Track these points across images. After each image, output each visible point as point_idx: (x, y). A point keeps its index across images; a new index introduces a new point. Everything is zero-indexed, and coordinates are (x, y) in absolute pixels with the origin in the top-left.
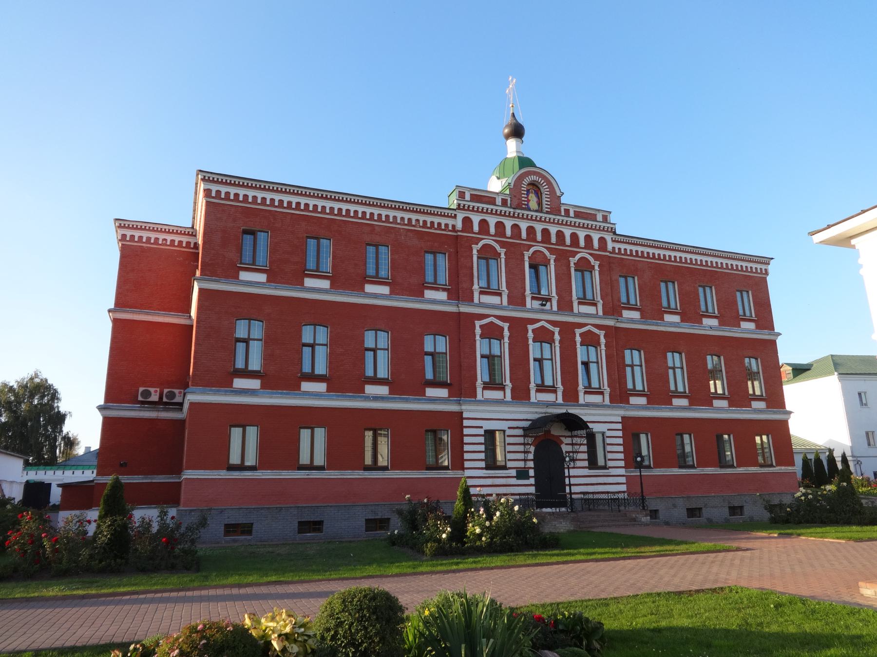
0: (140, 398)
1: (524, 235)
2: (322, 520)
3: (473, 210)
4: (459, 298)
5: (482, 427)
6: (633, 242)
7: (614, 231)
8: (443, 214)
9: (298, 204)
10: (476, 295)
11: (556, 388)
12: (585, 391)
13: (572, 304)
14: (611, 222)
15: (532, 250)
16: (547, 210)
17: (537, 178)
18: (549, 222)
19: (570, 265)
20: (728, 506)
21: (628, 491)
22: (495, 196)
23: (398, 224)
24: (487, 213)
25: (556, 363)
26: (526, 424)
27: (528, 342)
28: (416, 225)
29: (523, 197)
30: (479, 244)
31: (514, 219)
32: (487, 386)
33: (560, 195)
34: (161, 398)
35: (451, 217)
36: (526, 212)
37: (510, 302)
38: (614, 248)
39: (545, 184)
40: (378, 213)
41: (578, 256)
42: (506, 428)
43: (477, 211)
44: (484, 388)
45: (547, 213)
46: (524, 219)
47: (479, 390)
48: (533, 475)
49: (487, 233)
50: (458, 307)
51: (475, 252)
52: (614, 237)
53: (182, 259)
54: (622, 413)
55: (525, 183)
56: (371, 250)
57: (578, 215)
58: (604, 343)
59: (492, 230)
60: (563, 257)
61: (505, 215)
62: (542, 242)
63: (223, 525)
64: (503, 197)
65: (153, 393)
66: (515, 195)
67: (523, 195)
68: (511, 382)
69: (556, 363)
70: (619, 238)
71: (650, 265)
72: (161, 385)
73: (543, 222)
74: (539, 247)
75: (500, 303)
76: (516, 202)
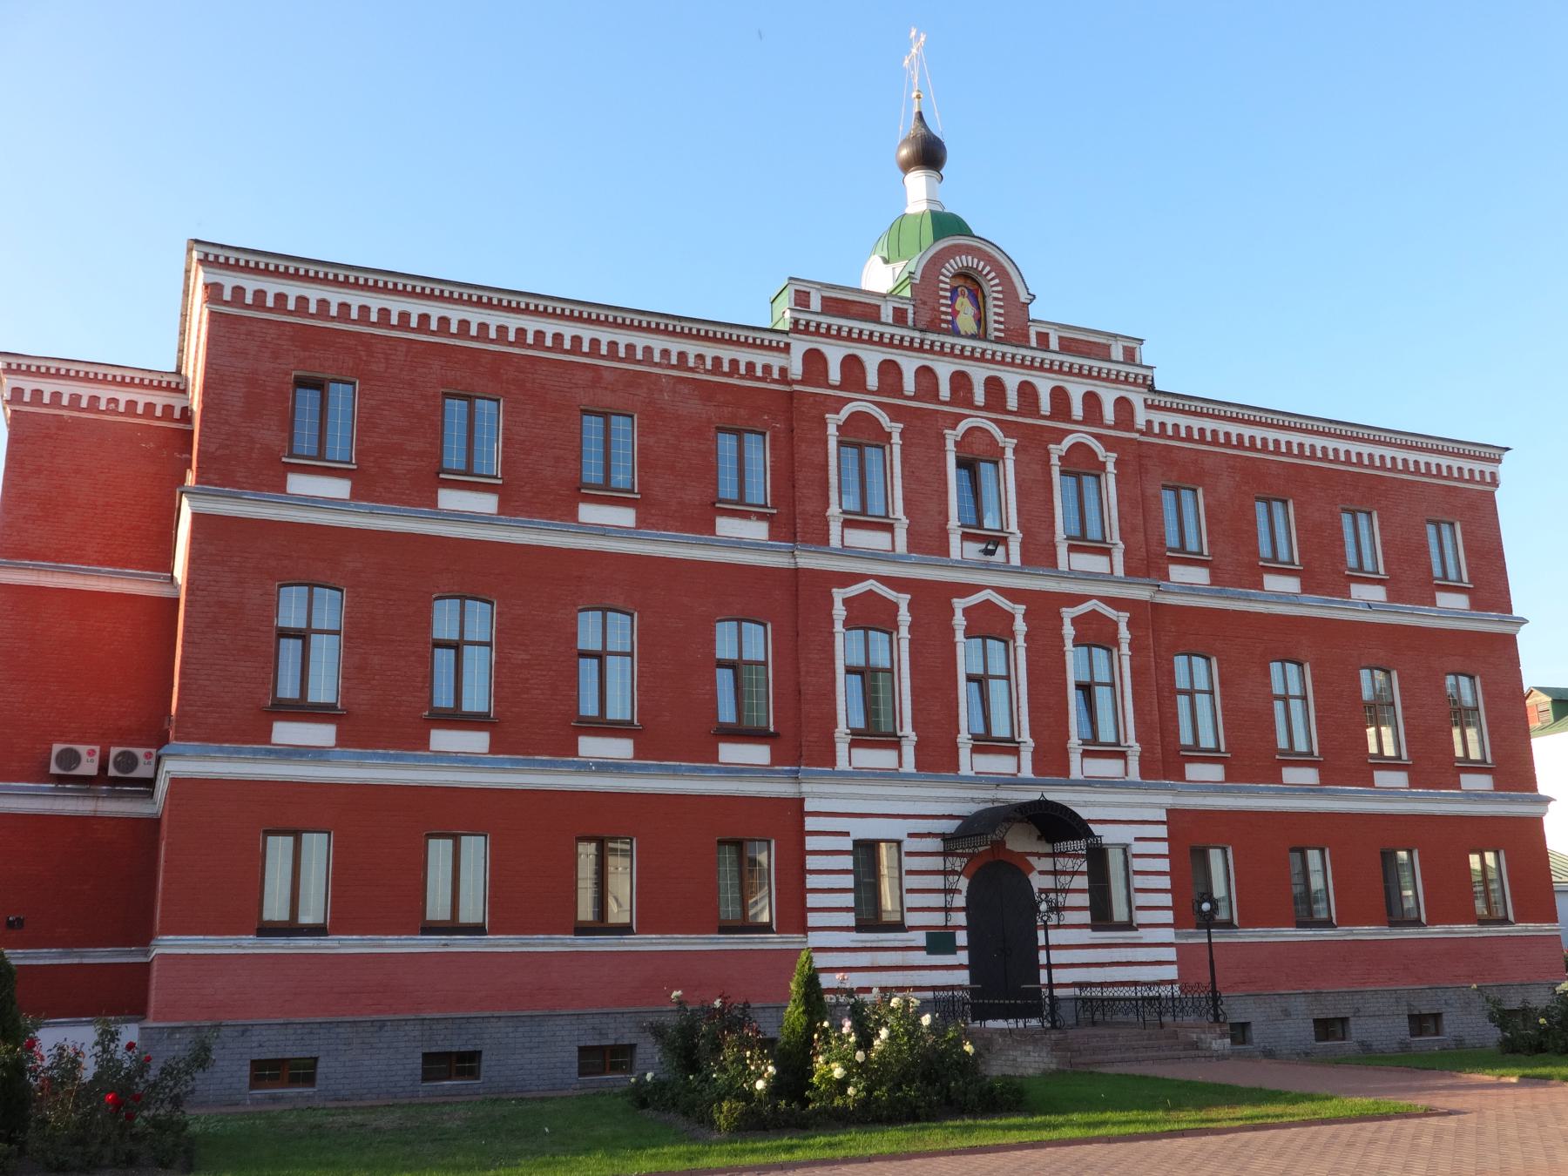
0: (54, 769)
1: (945, 391)
2: (479, 1049)
3: (828, 335)
4: (795, 536)
5: (847, 834)
6: (1193, 409)
7: (1149, 383)
8: (758, 342)
9: (424, 318)
10: (835, 529)
11: (1019, 743)
12: (1084, 750)
13: (1055, 550)
14: (1144, 364)
15: (963, 426)
16: (997, 334)
17: (976, 261)
18: (1003, 362)
19: (1049, 461)
20: (1407, 1012)
21: (1183, 981)
22: (878, 303)
23: (656, 365)
24: (860, 340)
25: (1017, 686)
26: (950, 826)
27: (954, 637)
28: (696, 368)
29: (943, 305)
30: (842, 412)
31: (921, 355)
32: (860, 739)
33: (1028, 301)
34: (103, 767)
35: (777, 349)
36: (949, 340)
37: (912, 546)
38: (1149, 423)
39: (993, 274)
40: (609, 340)
41: (1068, 441)
42: (903, 836)
43: (838, 336)
44: (854, 744)
45: (998, 340)
46: (945, 355)
47: (842, 749)
48: (965, 944)
49: (861, 386)
50: (794, 557)
51: (832, 430)
52: (1150, 397)
53: (152, 445)
54: (1169, 800)
55: (948, 274)
56: (593, 424)
57: (1067, 346)
58: (1128, 641)
59: (872, 380)
60: (1033, 443)
61: (901, 346)
62: (986, 408)
63: (249, 1062)
64: (896, 305)
65: (84, 756)
66: (923, 298)
67: (942, 301)
68: (914, 728)
69: (1017, 686)
70: (1162, 400)
71: (1231, 463)
72: (105, 738)
73: (987, 361)
74: (979, 419)
75: (890, 548)
76: (925, 317)
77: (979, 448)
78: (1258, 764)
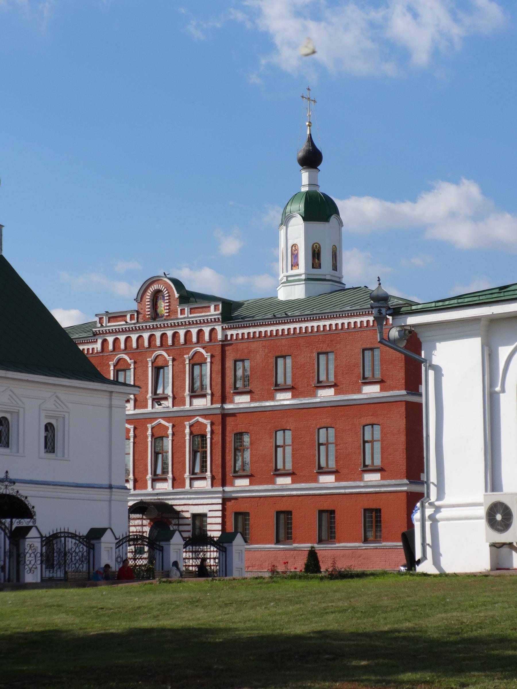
77: (160, 363)
78: (264, 477)
